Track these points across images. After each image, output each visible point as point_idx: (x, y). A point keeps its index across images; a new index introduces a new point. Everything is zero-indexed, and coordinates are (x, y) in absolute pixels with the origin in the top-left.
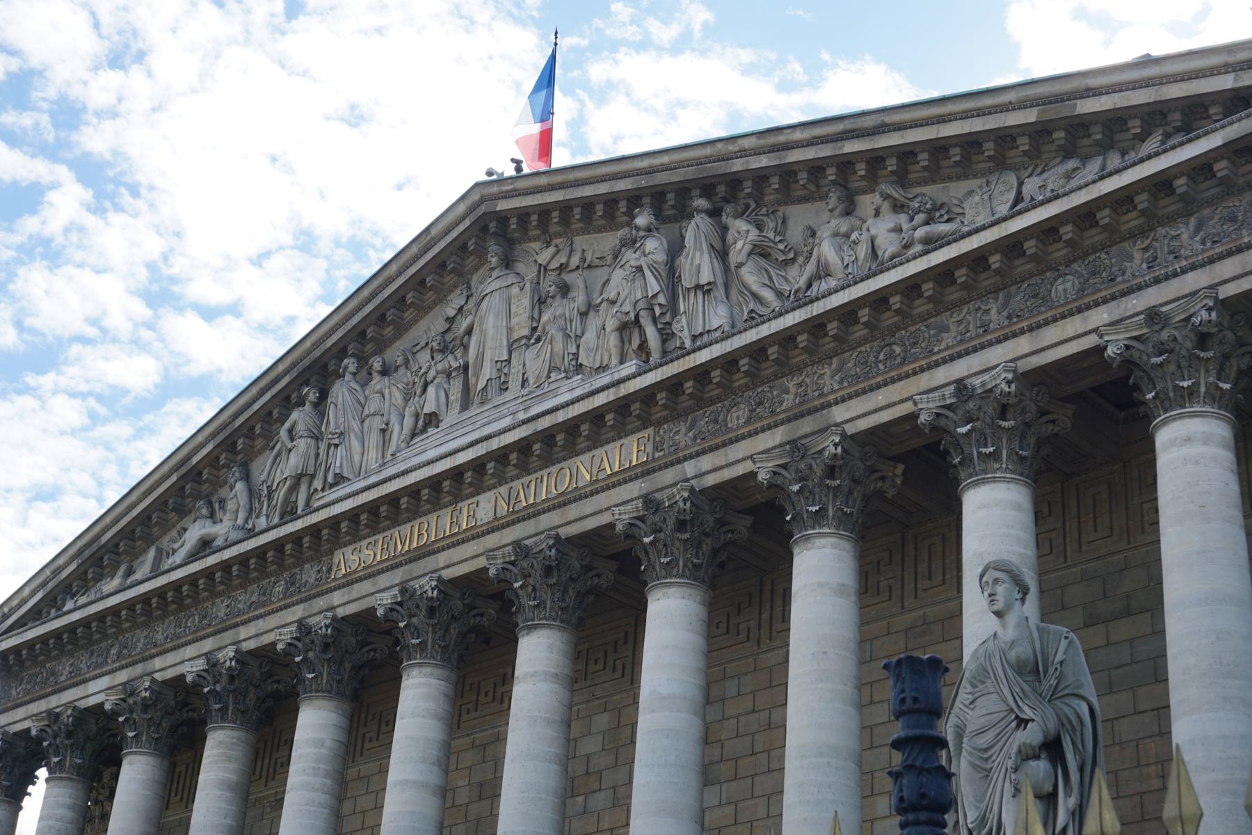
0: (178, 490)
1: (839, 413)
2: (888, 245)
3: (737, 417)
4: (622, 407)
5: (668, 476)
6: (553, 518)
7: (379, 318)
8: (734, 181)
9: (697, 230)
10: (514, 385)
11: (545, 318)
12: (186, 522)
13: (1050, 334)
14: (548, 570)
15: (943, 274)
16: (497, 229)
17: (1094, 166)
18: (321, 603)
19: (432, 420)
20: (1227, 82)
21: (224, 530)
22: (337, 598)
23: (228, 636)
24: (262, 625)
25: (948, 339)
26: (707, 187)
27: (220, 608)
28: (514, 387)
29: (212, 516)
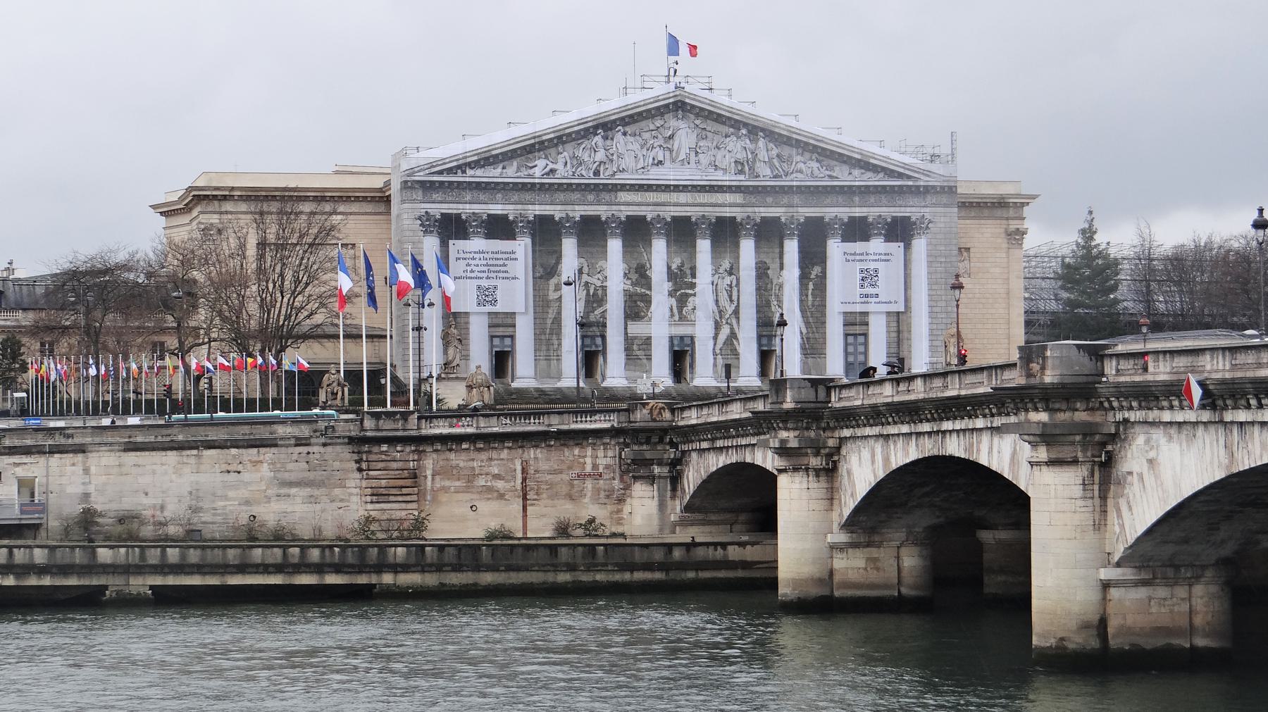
0: (533, 145)
1: (800, 210)
2: (816, 172)
3: (769, 200)
4: (738, 187)
5: (750, 209)
6: (710, 209)
7: (631, 116)
8: (772, 133)
9: (761, 143)
10: (692, 162)
11: (701, 143)
12: (530, 156)
13: (853, 209)
14: (710, 224)
15: (833, 187)
16: (679, 107)
17: (869, 174)
18: (614, 208)
19: (660, 162)
20: (901, 170)
21: (561, 167)
22: (622, 208)
23: (569, 207)
24: (586, 207)
25: (828, 201)
26: (763, 130)
27: (561, 196)
28: (693, 164)
29: (546, 158)
